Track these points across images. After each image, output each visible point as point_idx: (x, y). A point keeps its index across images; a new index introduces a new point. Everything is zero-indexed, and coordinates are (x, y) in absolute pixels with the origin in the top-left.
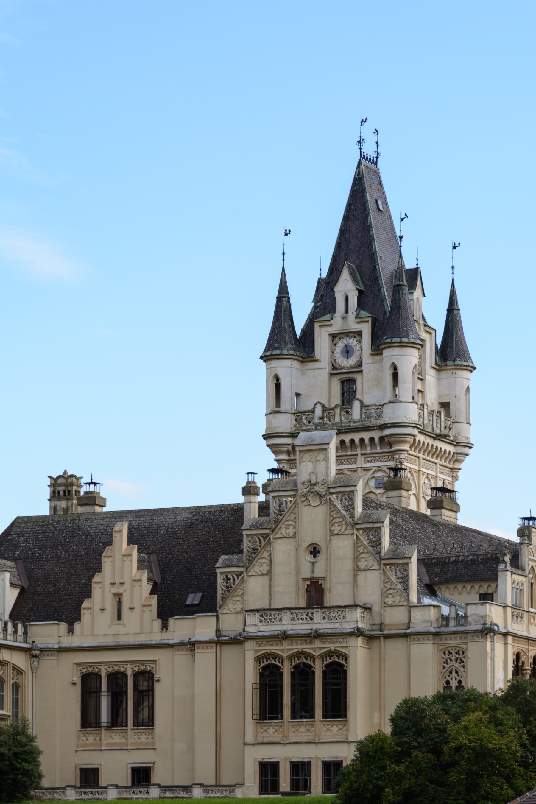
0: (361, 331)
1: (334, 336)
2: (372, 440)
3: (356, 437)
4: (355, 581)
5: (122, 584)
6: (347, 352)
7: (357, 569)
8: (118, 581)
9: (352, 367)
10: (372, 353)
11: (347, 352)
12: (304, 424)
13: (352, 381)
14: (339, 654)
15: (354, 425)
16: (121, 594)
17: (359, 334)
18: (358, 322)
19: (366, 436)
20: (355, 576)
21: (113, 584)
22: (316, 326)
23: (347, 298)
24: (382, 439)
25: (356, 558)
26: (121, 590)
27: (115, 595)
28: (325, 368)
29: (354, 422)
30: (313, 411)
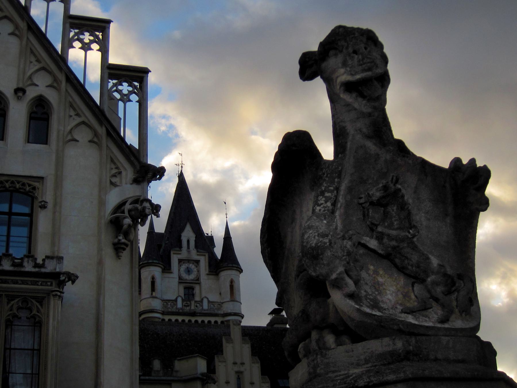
0: (199, 261)
1: (180, 261)
2: (216, 322)
3: (206, 319)
5: (243, 364)
6: (189, 271)
8: (239, 361)
10: (208, 273)
11: (189, 271)
12: (169, 307)
13: (193, 289)
15: (205, 312)
16: (241, 373)
17: (197, 262)
18: (198, 255)
19: (213, 319)
21: (235, 363)
22: (172, 252)
23: (188, 241)
24: (222, 322)
26: (242, 369)
27: (237, 372)
28: (177, 278)
29: (205, 310)
30: (176, 300)
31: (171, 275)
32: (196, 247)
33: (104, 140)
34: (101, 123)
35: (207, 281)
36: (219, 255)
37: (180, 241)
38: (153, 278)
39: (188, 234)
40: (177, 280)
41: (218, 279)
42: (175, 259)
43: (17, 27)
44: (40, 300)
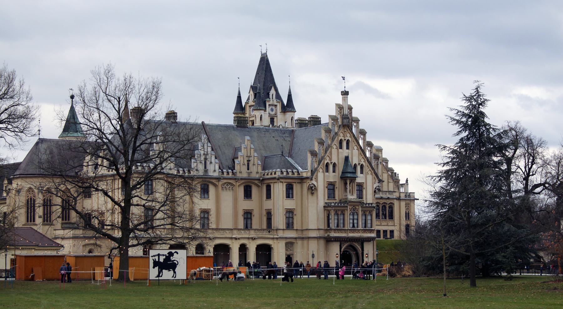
1: (269, 105)
4: (388, 185)
7: (388, 182)
9: (274, 114)
14: (391, 203)
17: (276, 106)
20: (388, 184)
25: (388, 180)
31: (266, 113)
32: (276, 98)
33: (373, 174)
34: (372, 170)
35: (280, 116)
36: (285, 104)
37: (268, 94)
38: (261, 116)
39: (273, 92)
40: (268, 115)
41: (285, 115)
42: (267, 104)
43: (358, 148)
44: (372, 211)
